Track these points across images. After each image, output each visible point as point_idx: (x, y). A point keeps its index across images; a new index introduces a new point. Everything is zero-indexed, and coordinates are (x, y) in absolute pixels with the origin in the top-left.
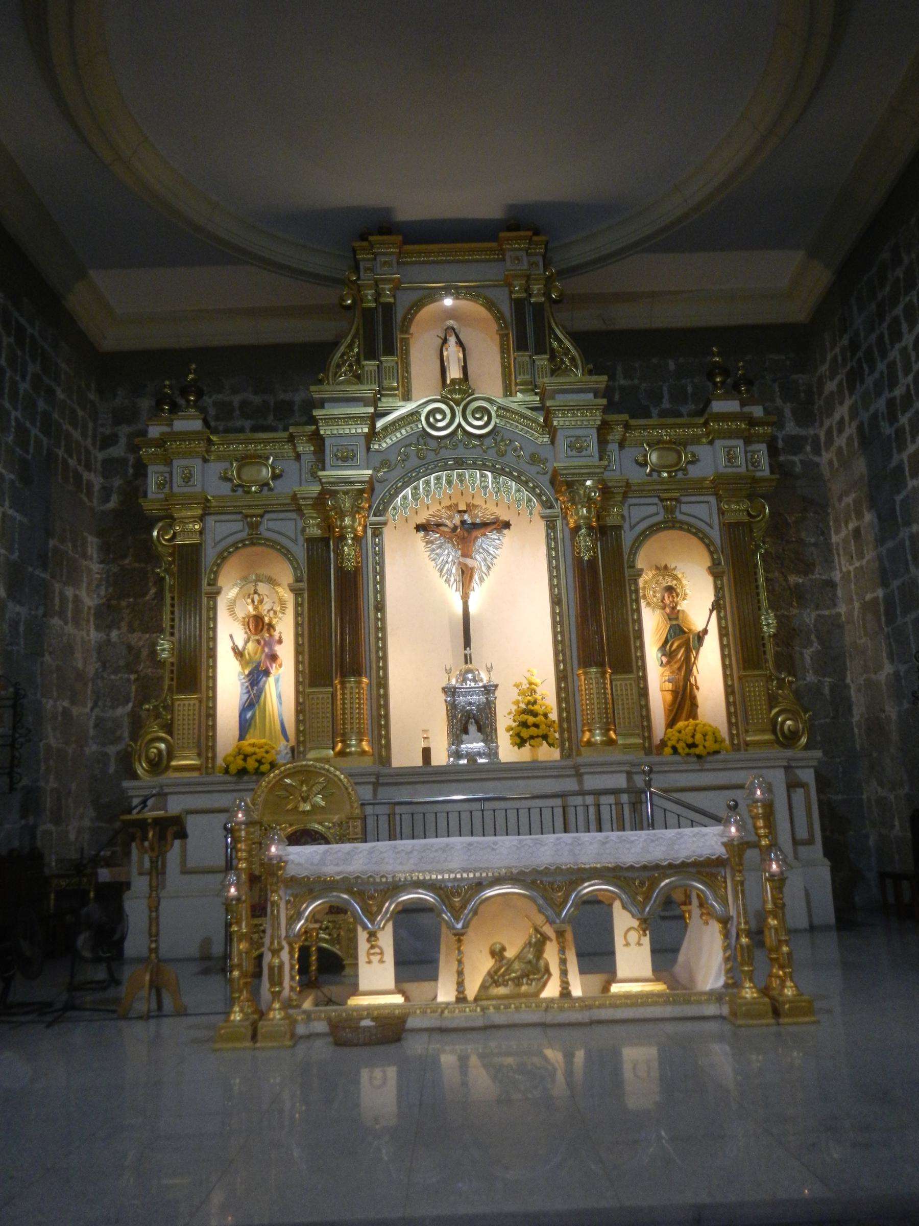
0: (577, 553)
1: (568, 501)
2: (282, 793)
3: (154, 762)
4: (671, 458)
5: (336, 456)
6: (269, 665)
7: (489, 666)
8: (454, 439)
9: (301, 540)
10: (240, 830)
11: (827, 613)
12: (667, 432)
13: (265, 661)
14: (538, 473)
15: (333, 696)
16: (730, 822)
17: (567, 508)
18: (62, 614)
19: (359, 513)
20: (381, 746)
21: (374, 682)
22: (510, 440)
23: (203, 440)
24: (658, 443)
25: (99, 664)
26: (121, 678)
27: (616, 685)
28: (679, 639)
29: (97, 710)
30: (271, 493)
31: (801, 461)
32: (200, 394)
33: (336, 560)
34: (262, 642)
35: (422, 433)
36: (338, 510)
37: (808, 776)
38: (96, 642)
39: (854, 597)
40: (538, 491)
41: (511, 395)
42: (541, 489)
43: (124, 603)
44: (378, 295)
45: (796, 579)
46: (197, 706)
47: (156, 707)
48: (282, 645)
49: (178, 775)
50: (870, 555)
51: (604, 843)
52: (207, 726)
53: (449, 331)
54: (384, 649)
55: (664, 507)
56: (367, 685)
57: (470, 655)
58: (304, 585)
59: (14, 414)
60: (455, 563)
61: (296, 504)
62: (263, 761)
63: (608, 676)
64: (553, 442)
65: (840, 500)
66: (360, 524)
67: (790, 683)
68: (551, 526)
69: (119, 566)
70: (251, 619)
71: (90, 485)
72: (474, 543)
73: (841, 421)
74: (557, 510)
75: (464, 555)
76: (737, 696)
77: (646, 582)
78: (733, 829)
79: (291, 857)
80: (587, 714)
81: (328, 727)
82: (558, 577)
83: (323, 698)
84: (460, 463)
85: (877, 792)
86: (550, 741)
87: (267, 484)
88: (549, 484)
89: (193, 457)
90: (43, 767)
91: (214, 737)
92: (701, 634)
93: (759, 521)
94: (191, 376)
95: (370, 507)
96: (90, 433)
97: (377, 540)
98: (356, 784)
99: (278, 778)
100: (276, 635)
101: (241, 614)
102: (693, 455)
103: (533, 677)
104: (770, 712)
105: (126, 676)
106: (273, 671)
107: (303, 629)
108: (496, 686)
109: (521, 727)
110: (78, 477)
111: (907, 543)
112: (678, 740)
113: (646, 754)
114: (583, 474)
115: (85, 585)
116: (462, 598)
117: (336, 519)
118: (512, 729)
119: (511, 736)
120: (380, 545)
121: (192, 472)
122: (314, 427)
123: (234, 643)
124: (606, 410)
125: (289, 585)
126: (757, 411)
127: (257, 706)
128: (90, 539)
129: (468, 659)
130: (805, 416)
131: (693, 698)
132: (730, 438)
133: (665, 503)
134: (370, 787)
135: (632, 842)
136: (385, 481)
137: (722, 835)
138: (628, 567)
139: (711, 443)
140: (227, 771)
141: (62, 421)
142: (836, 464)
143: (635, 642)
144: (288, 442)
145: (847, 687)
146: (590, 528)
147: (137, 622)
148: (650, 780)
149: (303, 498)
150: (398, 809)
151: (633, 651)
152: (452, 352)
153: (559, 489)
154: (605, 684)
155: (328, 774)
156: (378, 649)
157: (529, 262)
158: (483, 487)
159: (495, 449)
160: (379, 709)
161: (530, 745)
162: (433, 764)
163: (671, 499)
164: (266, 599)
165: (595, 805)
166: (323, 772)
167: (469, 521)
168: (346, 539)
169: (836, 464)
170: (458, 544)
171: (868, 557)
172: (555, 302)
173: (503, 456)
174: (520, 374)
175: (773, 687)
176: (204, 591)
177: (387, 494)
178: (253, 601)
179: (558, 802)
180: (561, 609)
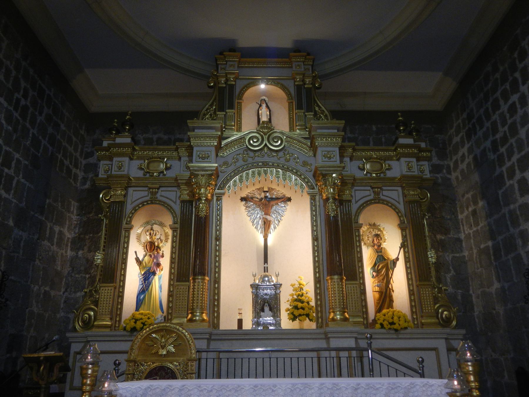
0: (328, 212)
1: (323, 184)
2: (150, 343)
3: (86, 322)
4: (378, 166)
5: (199, 156)
6: (155, 269)
7: (277, 273)
8: (263, 152)
9: (178, 202)
10: (87, 369)
11: (458, 255)
12: (375, 153)
13: (153, 266)
14: (306, 171)
16: (453, 377)
17: (323, 189)
18: (50, 239)
19: (209, 187)
20: (215, 317)
21: (213, 280)
22: (292, 154)
23: (130, 148)
24: (371, 158)
25: (71, 268)
26: (81, 277)
27: (348, 287)
28: (383, 263)
29: (66, 294)
30: (164, 176)
31: (441, 177)
32: (132, 126)
33: (196, 211)
34: (153, 256)
35: (246, 148)
36: (198, 184)
38: (70, 256)
39: (473, 247)
40: (306, 180)
41: (293, 131)
42: (308, 179)
43: (87, 237)
44: (227, 80)
45: (441, 236)
46: (112, 291)
47: (91, 291)
48: (164, 258)
49: (97, 330)
50: (482, 224)
51: (356, 389)
52: (118, 302)
53: (262, 101)
54: (219, 262)
55: (373, 192)
56: (208, 281)
57: (267, 267)
58: (178, 226)
59: (31, 131)
60: (261, 218)
61: (177, 183)
62: (146, 323)
63: (344, 281)
64: (315, 156)
65: (463, 196)
66: (209, 193)
67: (445, 290)
68: (313, 198)
69: (87, 217)
70: (148, 244)
71: (76, 176)
72: (272, 208)
73: (463, 155)
74: (316, 190)
75: (266, 214)
76: (415, 296)
77: (364, 232)
78: (456, 383)
79: (120, 391)
80: (332, 302)
81: (185, 305)
82: (316, 226)
83: (184, 288)
84: (265, 165)
85: (492, 356)
86: (311, 318)
87: (163, 172)
88: (312, 177)
89: (124, 157)
90: (27, 323)
91: (121, 309)
92: (395, 261)
93: (424, 202)
94: (128, 117)
95: (216, 185)
96: (79, 150)
97: (219, 203)
98: (195, 339)
99: (148, 333)
100: (161, 252)
101: (143, 240)
102: (389, 165)
103: (302, 281)
104: (435, 307)
105: (84, 275)
106: (158, 273)
107: (176, 250)
108: (281, 285)
109: (294, 309)
110: (69, 171)
111: (507, 216)
112: (384, 321)
113: (365, 328)
114: (331, 170)
115: (67, 226)
116: (264, 237)
117: (197, 189)
118: (289, 310)
119: (288, 314)
120: (220, 205)
121: (123, 164)
122: (189, 143)
123: (137, 256)
124: (344, 140)
125: (170, 225)
126: (423, 145)
127: (147, 292)
128: (73, 202)
130: (443, 154)
131: (391, 297)
132: (409, 157)
133: (374, 190)
134: (206, 341)
135: (377, 389)
136: (225, 172)
137: (446, 386)
138: (354, 223)
139: (398, 160)
140: (125, 329)
141: (62, 141)
142: (460, 178)
143: (358, 264)
144: (175, 151)
145: (471, 296)
146: (334, 199)
147: (93, 247)
148: (371, 343)
149: (180, 179)
150: (222, 355)
151: (357, 269)
153: (318, 179)
154: (342, 285)
155: (178, 332)
156: (216, 261)
157: (304, 68)
158: (277, 177)
159: (284, 158)
160: (214, 296)
161: (299, 320)
162: (243, 329)
163: (378, 188)
164: (157, 233)
165: (336, 357)
166: (175, 330)
167: (269, 197)
168: (201, 200)
169: (460, 178)
170: (263, 209)
171: (481, 225)
172: (318, 88)
173: (288, 161)
174: (298, 121)
175: (435, 292)
176: (123, 227)
177: (226, 179)
178: (150, 234)
179: (314, 354)
180: (318, 242)
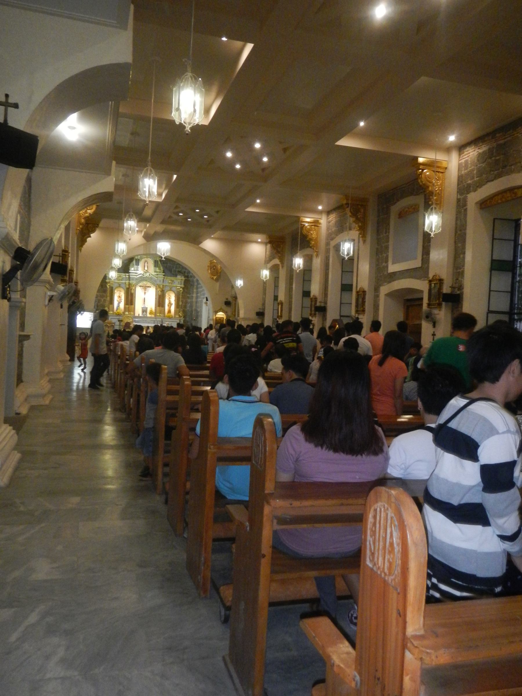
15: (129, 307)
37: (182, 321)
68: (156, 289)
129: (144, 304)
146: (161, 291)
152: (146, 264)
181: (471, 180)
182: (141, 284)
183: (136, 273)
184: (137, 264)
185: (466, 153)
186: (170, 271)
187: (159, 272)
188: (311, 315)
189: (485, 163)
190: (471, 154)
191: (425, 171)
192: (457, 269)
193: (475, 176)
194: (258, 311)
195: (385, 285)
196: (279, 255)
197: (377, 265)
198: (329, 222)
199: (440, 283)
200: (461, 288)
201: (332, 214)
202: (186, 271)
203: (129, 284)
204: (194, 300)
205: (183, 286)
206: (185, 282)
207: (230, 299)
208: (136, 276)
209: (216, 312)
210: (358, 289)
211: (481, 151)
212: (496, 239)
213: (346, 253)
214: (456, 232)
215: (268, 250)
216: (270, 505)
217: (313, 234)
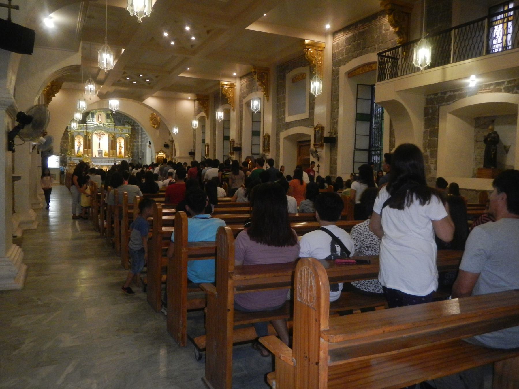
15: (87, 150)
37: (131, 160)
68: (109, 136)
84: (100, 129)
181: (341, 56)
182: (96, 132)
183: (92, 124)
184: (93, 116)
185: (337, 37)
186: (120, 122)
187: (111, 123)
188: (230, 153)
189: (351, 45)
190: (341, 38)
191: (310, 49)
192: (333, 120)
193: (344, 54)
194: (190, 151)
195: (283, 131)
196: (205, 109)
197: (277, 117)
198: (242, 85)
199: (322, 130)
200: (336, 133)
201: (244, 79)
202: (133, 121)
203: (87, 132)
204: (140, 144)
205: (130, 133)
206: (131, 131)
207: (168, 143)
208: (92, 126)
209: (158, 153)
210: (264, 134)
211: (347, 36)
212: (359, 99)
213: (255, 109)
214: (332, 94)
215: (196, 106)
216: (232, 279)
217: (230, 94)
